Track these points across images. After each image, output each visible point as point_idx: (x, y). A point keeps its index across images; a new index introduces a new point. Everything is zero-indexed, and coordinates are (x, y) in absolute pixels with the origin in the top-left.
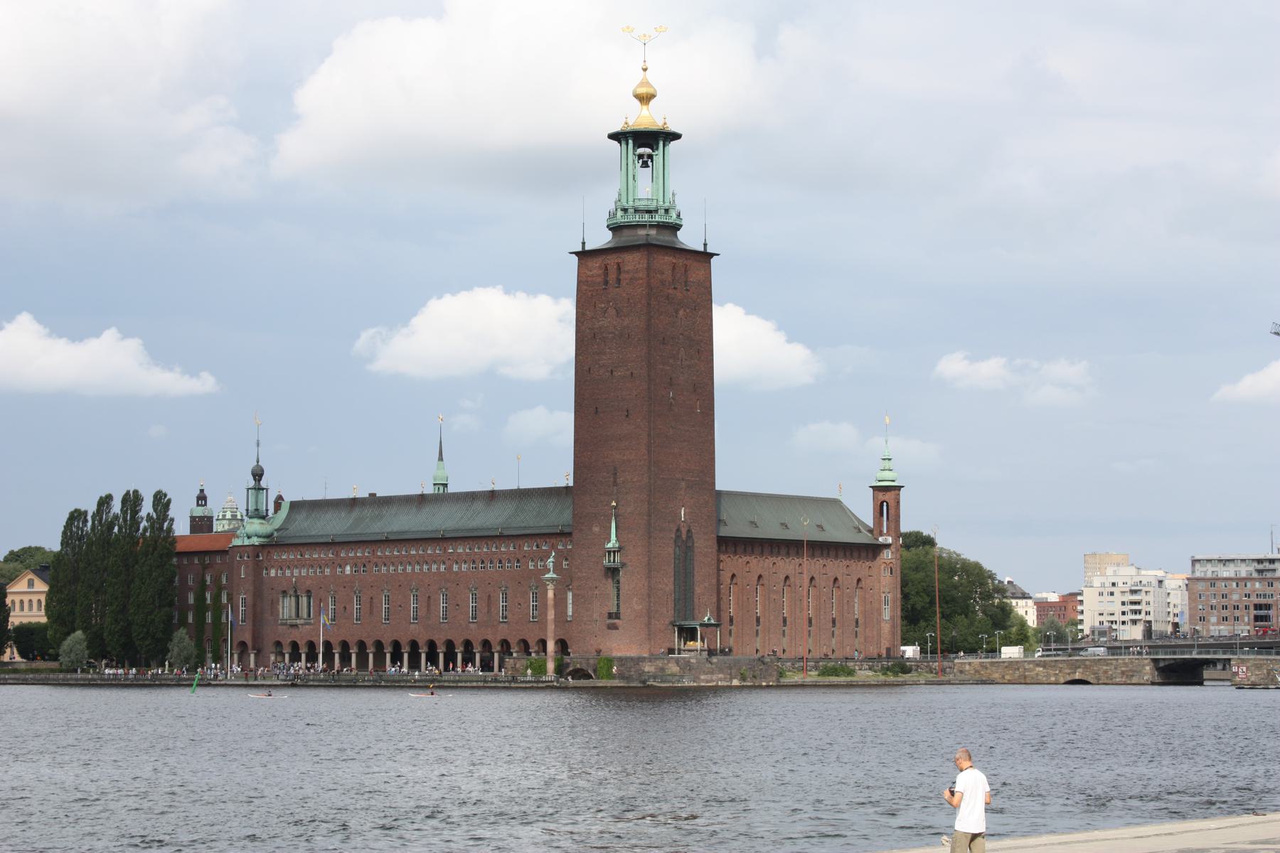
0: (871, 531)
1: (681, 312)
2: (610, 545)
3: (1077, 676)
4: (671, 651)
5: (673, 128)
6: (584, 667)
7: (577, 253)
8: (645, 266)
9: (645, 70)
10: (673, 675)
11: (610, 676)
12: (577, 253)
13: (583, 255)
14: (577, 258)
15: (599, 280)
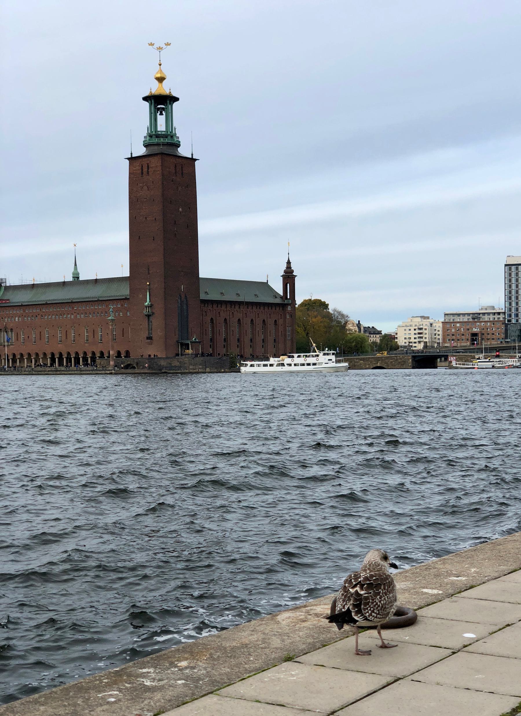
0: (281, 297)
1: (180, 188)
2: (146, 304)
3: (379, 365)
4: (177, 355)
5: (174, 94)
6: (132, 363)
7: (128, 159)
8: (160, 164)
9: (160, 65)
10: (175, 366)
11: (144, 367)
12: (128, 159)
13: (132, 159)
14: (127, 162)
15: (140, 171)
